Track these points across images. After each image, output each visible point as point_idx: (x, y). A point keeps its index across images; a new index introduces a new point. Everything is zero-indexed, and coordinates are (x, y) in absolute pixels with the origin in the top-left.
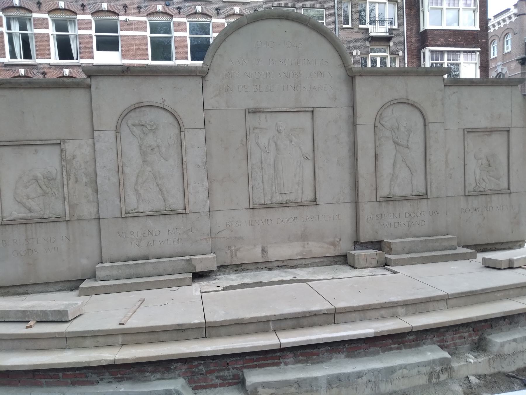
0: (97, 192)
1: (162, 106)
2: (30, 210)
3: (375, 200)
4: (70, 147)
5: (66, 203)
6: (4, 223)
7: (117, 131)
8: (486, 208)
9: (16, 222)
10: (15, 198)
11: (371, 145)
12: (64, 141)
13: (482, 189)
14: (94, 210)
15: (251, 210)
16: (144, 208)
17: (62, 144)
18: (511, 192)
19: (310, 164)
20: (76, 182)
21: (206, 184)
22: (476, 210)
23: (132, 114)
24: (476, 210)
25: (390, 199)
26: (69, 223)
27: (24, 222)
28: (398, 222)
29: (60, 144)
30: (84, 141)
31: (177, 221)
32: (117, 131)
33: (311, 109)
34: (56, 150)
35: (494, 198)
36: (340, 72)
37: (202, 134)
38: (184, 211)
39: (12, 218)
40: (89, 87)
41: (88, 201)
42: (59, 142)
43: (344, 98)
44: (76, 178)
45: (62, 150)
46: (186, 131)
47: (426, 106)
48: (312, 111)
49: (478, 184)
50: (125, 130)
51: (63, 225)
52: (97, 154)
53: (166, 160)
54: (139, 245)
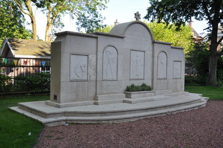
4: (90, 57)
5: (88, 75)
6: (72, 81)
10: (75, 72)
11: (157, 63)
14: (95, 78)
16: (108, 79)
19: (143, 67)
20: (91, 68)
25: (160, 79)
30: (94, 55)
34: (86, 57)
36: (150, 41)
39: (74, 79)
40: (97, 38)
41: (94, 75)
43: (151, 49)
44: (91, 67)
47: (167, 53)
50: (105, 52)
51: (87, 82)
52: (98, 60)
53: (113, 63)
54: (106, 90)
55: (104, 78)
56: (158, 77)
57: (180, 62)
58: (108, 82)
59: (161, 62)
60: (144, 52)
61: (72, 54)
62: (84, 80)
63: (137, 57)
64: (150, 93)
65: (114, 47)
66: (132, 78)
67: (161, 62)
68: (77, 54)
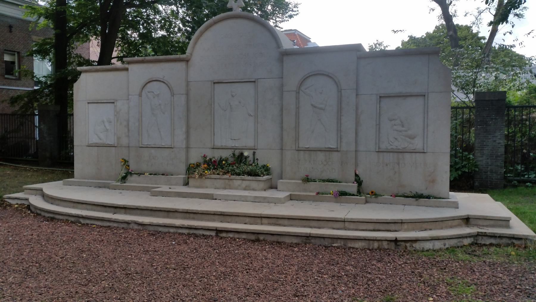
0: (129, 130)
1: (162, 80)
2: (100, 139)
3: (294, 149)
7: (140, 95)
8: (398, 164)
9: (94, 145)
12: (116, 100)
13: (395, 148)
15: (213, 149)
17: (115, 102)
18: (425, 151)
20: (121, 124)
21: (184, 129)
22: (387, 165)
23: (148, 85)
24: (387, 165)
26: (117, 148)
27: (97, 145)
28: (313, 168)
29: (113, 103)
31: (166, 152)
32: (140, 95)
33: (253, 80)
35: (407, 156)
37: (183, 98)
38: (171, 147)
42: (113, 101)
45: (115, 106)
46: (175, 95)
48: (254, 82)
49: (390, 143)
53: (164, 113)
55: (145, 142)
56: (303, 144)
57: (420, 100)
58: (153, 151)
59: (312, 105)
60: (253, 84)
61: (89, 102)
62: (109, 145)
63: (233, 96)
64: (244, 182)
65: (164, 82)
66: (218, 144)
67: (312, 105)
68: (96, 101)
